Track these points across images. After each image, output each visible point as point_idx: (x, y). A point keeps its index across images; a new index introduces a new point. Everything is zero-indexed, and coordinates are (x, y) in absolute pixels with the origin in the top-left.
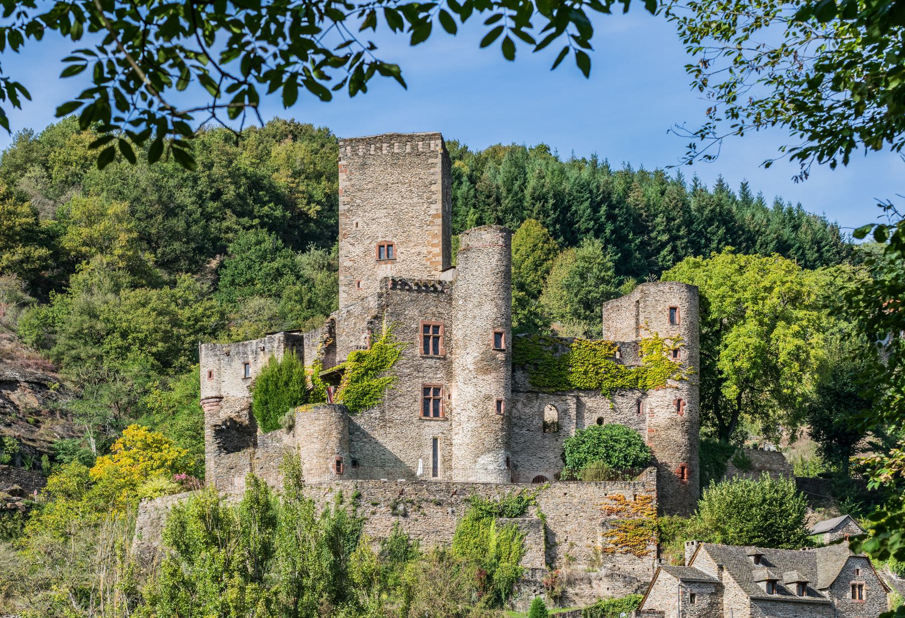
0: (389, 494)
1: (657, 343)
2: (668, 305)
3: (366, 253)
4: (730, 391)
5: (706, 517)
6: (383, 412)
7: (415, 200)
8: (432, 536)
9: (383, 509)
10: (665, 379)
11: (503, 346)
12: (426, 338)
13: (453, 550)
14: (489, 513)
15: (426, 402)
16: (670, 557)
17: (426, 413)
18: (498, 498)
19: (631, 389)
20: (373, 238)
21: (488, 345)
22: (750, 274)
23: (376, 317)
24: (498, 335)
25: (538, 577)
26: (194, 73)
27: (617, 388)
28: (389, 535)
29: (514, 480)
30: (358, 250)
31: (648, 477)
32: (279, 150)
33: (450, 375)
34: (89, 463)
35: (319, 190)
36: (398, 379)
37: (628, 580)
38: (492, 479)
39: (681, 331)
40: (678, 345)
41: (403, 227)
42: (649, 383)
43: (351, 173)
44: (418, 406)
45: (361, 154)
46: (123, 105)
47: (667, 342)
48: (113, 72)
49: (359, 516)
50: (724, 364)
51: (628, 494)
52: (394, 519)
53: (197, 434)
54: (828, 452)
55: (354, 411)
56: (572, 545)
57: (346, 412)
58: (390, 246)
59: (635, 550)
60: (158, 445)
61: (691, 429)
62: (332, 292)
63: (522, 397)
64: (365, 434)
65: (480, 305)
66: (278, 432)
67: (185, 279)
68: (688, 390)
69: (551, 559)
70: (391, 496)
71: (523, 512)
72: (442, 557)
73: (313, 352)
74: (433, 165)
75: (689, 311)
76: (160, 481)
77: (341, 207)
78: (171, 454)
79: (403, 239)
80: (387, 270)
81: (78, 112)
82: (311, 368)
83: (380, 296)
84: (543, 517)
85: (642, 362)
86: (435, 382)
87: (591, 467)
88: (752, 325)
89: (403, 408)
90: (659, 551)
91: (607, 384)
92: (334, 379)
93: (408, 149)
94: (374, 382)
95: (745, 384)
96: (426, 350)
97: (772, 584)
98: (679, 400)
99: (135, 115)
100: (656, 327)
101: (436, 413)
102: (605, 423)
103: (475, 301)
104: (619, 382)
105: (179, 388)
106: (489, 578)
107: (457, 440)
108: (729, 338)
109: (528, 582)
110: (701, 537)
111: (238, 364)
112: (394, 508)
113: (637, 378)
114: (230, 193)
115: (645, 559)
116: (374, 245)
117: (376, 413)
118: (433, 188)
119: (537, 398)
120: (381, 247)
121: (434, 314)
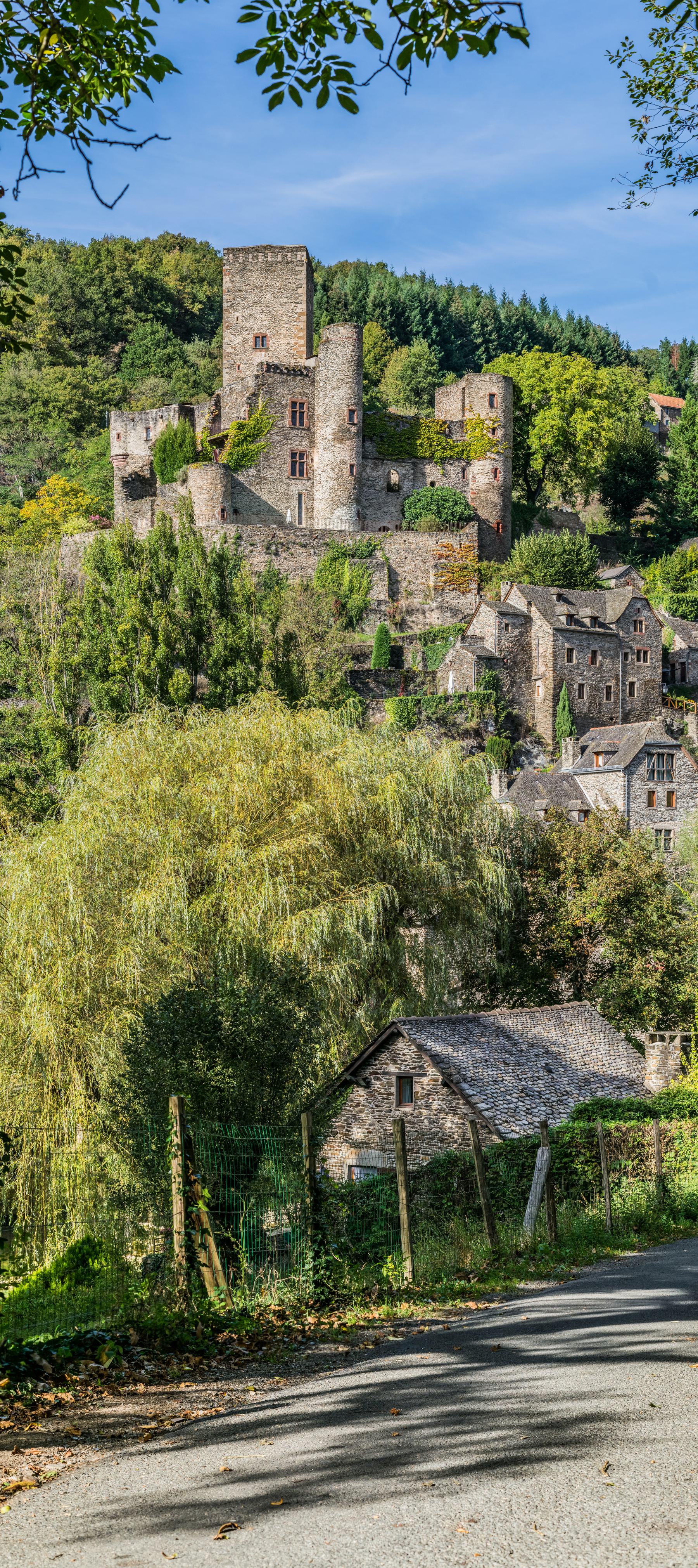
0: (263, 537)
1: (479, 422)
2: (488, 392)
3: (245, 342)
4: (537, 463)
5: (517, 564)
6: (258, 471)
9: (259, 549)
11: (356, 421)
13: (315, 583)
14: (344, 554)
15: (293, 464)
16: (488, 594)
17: (293, 473)
18: (351, 542)
19: (458, 459)
20: (250, 330)
22: (554, 369)
23: (253, 394)
24: (352, 412)
25: (383, 607)
26: (361, 27)
28: (263, 569)
29: (363, 529)
30: (238, 339)
31: (471, 529)
32: (170, 259)
33: (312, 443)
34: (19, 504)
35: (203, 291)
36: (271, 444)
37: (455, 612)
38: (346, 527)
39: (497, 413)
41: (274, 321)
42: (472, 454)
44: (287, 467)
46: (293, 55)
47: (487, 422)
48: (285, 23)
49: (240, 554)
50: (533, 442)
51: (455, 543)
52: (267, 557)
53: (106, 485)
54: (615, 515)
55: (235, 470)
56: (410, 582)
57: (230, 470)
58: (264, 337)
59: (460, 587)
60: (75, 493)
61: (505, 493)
62: (217, 373)
63: (370, 463)
64: (244, 488)
65: (337, 387)
66: (174, 485)
67: (94, 361)
68: (504, 461)
69: (393, 593)
70: (266, 538)
71: (371, 555)
72: (306, 588)
73: (203, 421)
74: (300, 272)
75: (505, 398)
76: (76, 521)
77: (225, 304)
78: (85, 501)
79: (274, 331)
80: (261, 357)
81: (256, 59)
82: (201, 433)
83: (257, 377)
84: (387, 559)
85: (467, 437)
86: (300, 448)
87: (427, 519)
88: (555, 410)
90: (479, 590)
91: (438, 455)
92: (219, 443)
93: (279, 258)
94: (252, 447)
95: (547, 458)
96: (294, 423)
97: (571, 617)
99: (305, 65)
100: (478, 409)
101: (301, 474)
102: (437, 485)
103: (333, 384)
104: (448, 453)
105: (91, 447)
106: (344, 606)
107: (317, 495)
108: (537, 420)
109: (375, 611)
110: (513, 579)
111: (141, 428)
112: (268, 548)
113: (463, 451)
114: (130, 292)
115: (468, 595)
116: (251, 335)
117: (253, 472)
118: (300, 291)
120: (256, 337)
121: (300, 394)
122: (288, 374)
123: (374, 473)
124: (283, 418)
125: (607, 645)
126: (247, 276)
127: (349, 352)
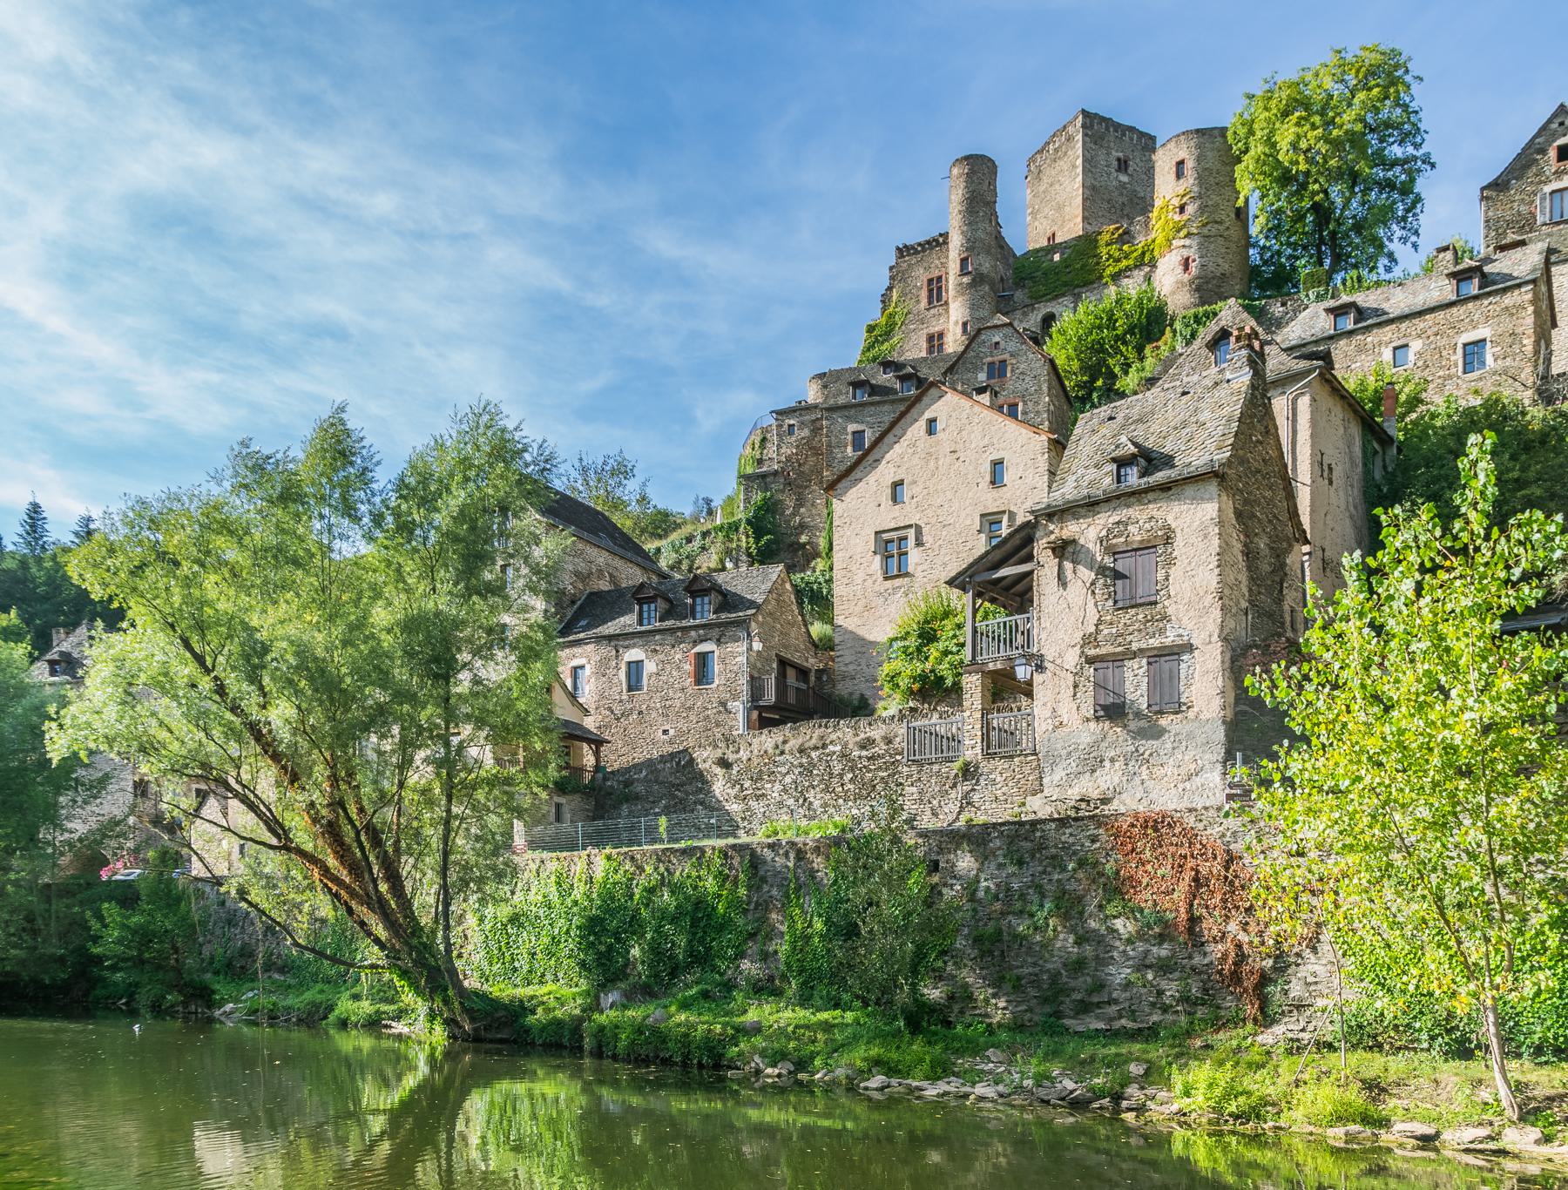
10: (1169, 241)
12: (930, 291)
19: (1136, 267)
23: (890, 289)
27: (1120, 271)
36: (907, 334)
40: (1185, 199)
75: (1199, 159)
85: (1153, 236)
94: (886, 345)
98: (1187, 259)
104: (1125, 263)
122: (924, 250)
124: (918, 302)
127: (960, 192)
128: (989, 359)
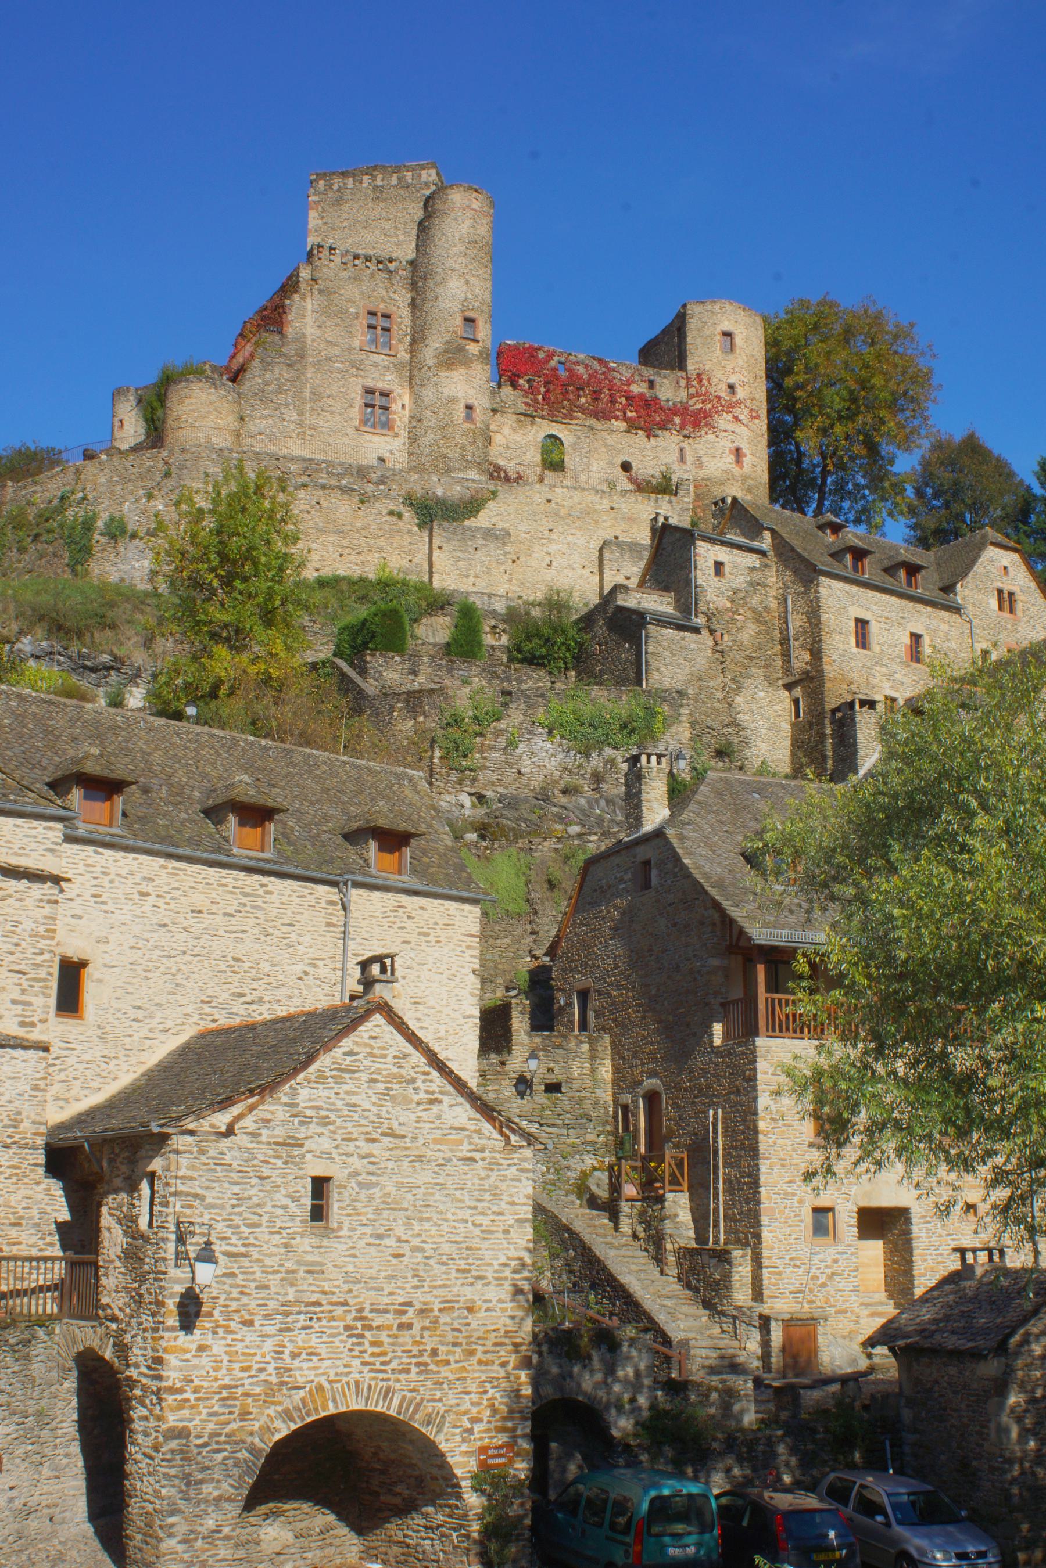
7: (401, 237)
8: (334, 538)
21: (455, 332)
43: (324, 211)
44: (355, 413)
45: (335, 187)
86: (380, 385)
89: (332, 413)
119: (533, 423)
123: (518, 437)
125: (944, 627)
126: (345, 208)
128: (999, 585)
